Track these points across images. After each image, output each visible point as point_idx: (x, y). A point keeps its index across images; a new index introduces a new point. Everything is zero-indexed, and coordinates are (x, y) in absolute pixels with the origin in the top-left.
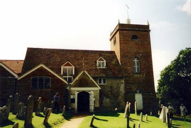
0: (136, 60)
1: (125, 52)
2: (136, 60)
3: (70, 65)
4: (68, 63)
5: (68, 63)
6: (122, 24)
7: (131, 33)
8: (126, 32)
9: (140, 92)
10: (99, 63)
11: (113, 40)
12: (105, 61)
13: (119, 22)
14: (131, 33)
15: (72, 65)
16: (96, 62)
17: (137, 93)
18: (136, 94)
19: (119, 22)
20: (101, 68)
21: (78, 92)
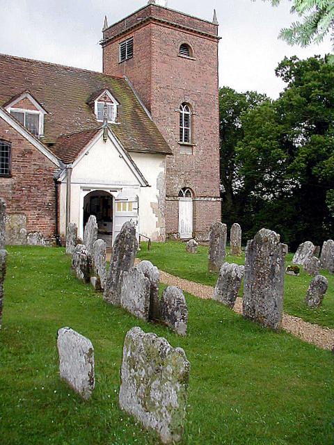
3: (31, 107)
4: (26, 98)
8: (167, 30)
11: (117, 47)
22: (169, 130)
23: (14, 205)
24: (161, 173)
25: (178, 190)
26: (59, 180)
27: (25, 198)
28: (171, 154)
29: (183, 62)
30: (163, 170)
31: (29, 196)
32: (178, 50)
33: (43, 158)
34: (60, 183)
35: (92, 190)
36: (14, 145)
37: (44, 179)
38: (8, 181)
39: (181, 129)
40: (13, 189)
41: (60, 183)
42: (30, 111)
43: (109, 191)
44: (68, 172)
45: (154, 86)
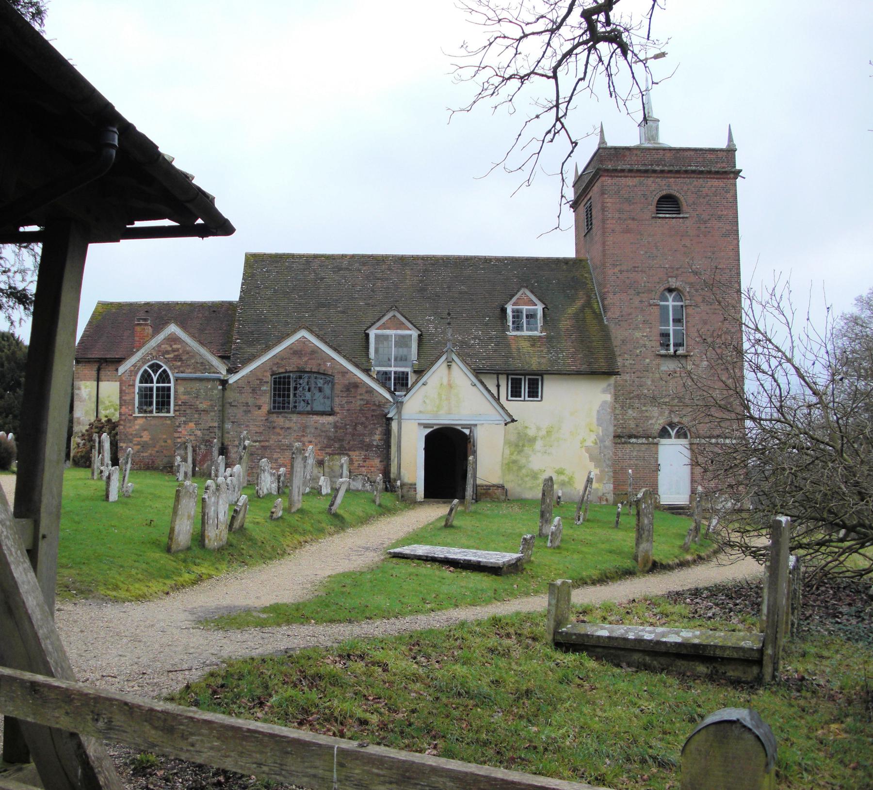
0: (671, 299)
1: (624, 268)
2: (671, 299)
3: (401, 326)
4: (394, 316)
5: (394, 316)
6: (616, 149)
7: (657, 187)
8: (630, 181)
9: (681, 434)
10: (517, 314)
11: (582, 209)
12: (539, 308)
13: (602, 140)
14: (657, 187)
15: (410, 325)
16: (504, 311)
17: (670, 436)
18: (663, 441)
19: (602, 140)
20: (526, 333)
21: (429, 430)
22: (638, 334)
23: (337, 445)
24: (605, 402)
25: (658, 427)
26: (389, 416)
27: (349, 437)
28: (617, 373)
29: (668, 224)
30: (608, 398)
31: (353, 435)
32: (653, 208)
33: (370, 391)
34: (391, 419)
35: (435, 427)
36: (338, 378)
37: (372, 416)
38: (331, 419)
39: (666, 335)
40: (336, 427)
41: (391, 419)
42: (400, 332)
43: (459, 428)
44: (399, 405)
45: (610, 272)
